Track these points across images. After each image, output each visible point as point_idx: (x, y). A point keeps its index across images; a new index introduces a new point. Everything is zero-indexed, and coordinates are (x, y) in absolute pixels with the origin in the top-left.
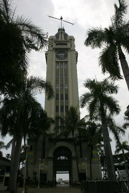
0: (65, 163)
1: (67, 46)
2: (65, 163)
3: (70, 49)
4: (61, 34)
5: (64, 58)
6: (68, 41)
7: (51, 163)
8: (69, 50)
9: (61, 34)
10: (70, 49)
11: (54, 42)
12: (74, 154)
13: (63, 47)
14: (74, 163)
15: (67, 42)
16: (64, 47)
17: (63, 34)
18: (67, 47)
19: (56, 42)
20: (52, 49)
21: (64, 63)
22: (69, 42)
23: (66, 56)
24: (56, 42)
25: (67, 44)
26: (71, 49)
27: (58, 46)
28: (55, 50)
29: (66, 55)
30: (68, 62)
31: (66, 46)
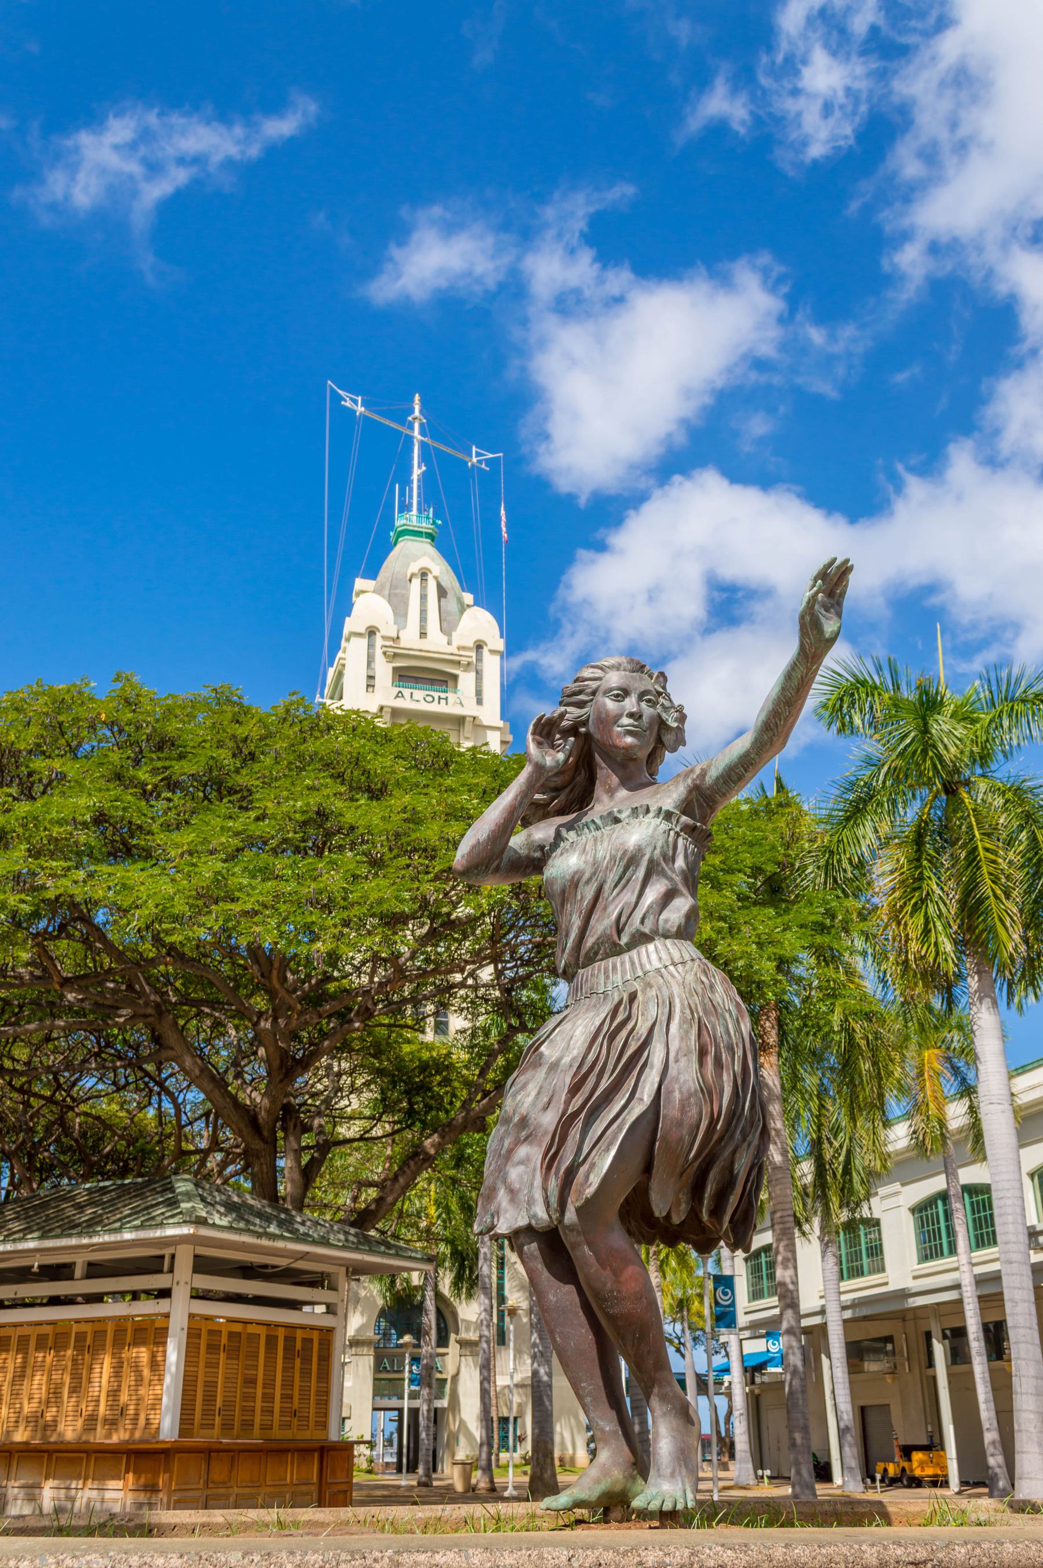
8: (468, 726)
11: (385, 653)
18: (458, 711)
19: (395, 655)
25: (455, 678)
31: (450, 696)
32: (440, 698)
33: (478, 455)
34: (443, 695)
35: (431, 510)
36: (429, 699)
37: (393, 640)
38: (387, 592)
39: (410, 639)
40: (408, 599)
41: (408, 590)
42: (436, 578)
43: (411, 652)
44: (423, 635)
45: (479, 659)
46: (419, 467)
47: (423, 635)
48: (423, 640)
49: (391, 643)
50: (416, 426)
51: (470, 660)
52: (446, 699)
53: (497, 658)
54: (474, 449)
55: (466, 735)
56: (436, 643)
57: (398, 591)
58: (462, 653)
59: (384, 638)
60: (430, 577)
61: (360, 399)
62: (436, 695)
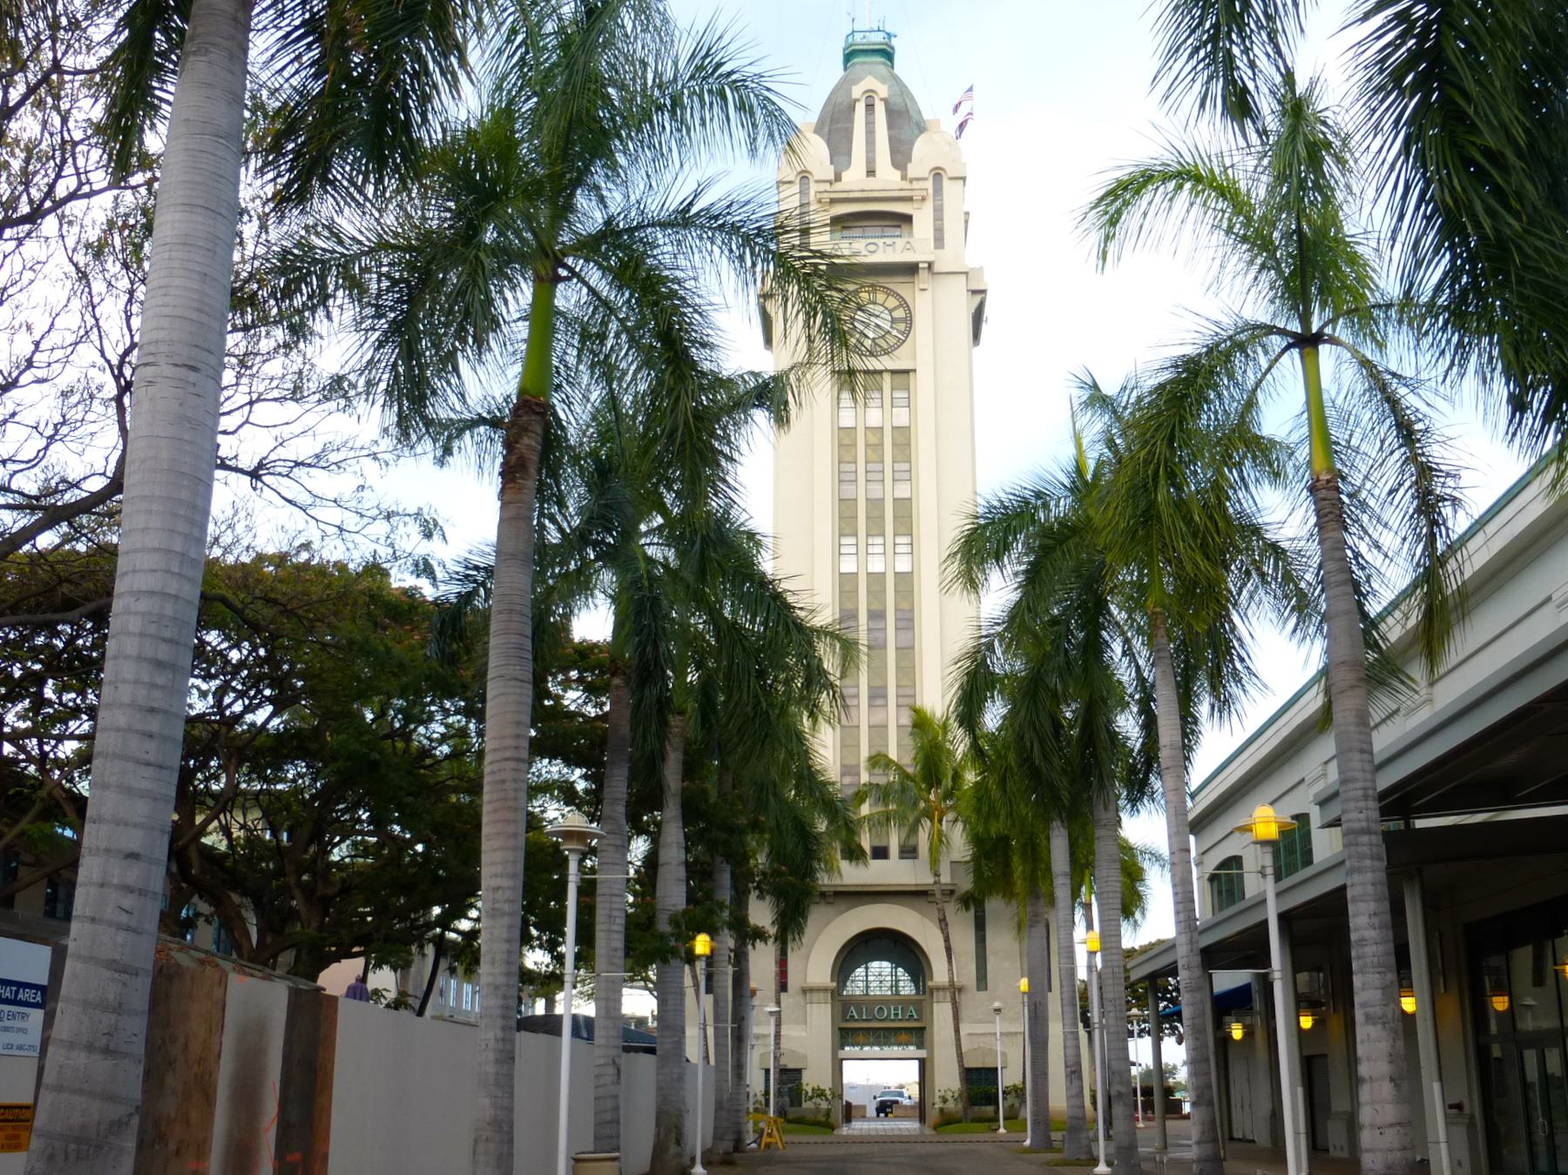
0: (896, 1015)
1: (909, 247)
2: (896, 1015)
3: (930, 265)
4: (870, 107)
6: (917, 195)
7: (821, 1016)
8: (923, 274)
9: (870, 107)
10: (930, 265)
12: (940, 973)
14: (941, 1013)
15: (910, 199)
17: (880, 109)
19: (833, 201)
21: (887, 377)
22: (923, 199)
24: (833, 201)
25: (908, 219)
26: (936, 268)
29: (900, 313)
30: (915, 371)
31: (900, 242)
34: (889, 241)
36: (872, 248)
37: (831, 183)
38: (826, 130)
39: (854, 178)
40: (851, 133)
41: (851, 121)
42: (885, 100)
43: (852, 195)
44: (871, 172)
45: (938, 190)
47: (871, 172)
48: (871, 179)
49: (827, 187)
51: (924, 193)
56: (888, 178)
57: (840, 125)
58: (916, 185)
59: (817, 182)
62: (880, 242)
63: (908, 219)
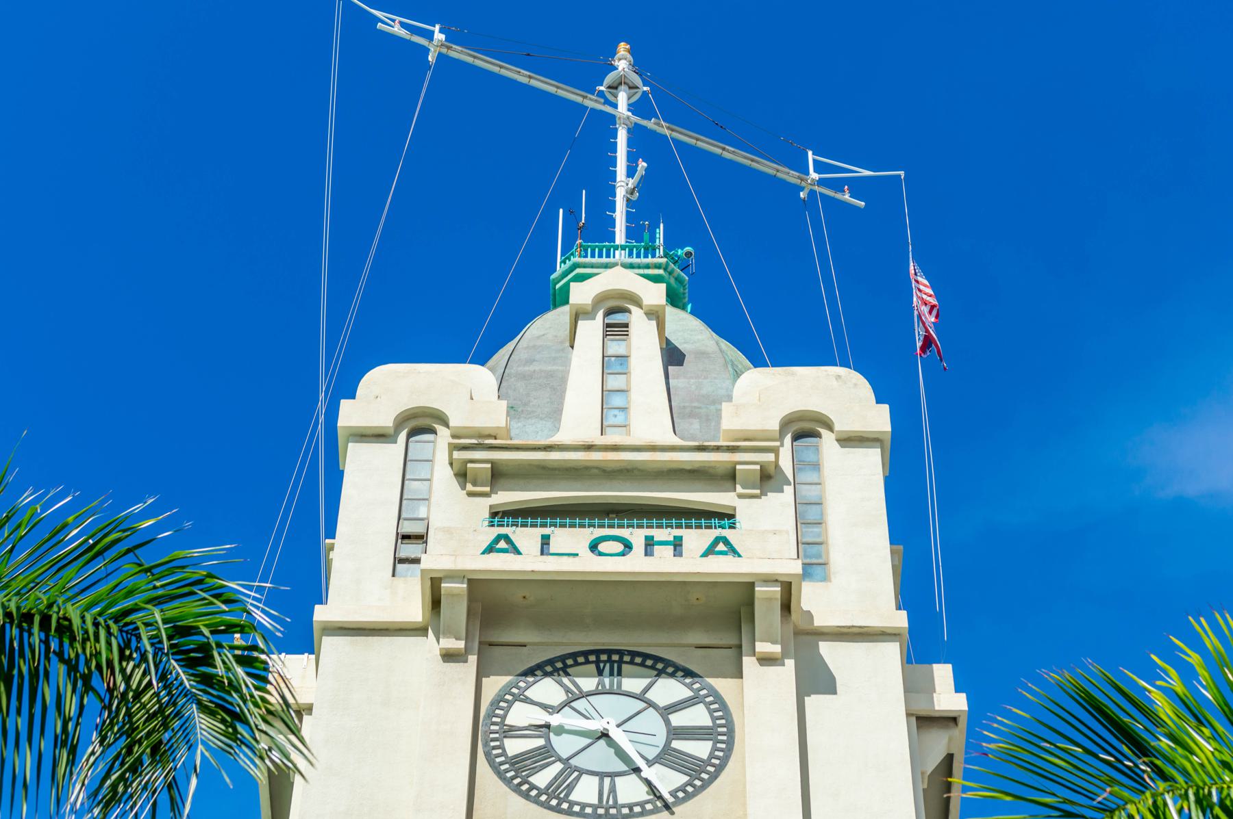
5: (668, 780)
11: (462, 475)
13: (636, 564)
15: (729, 477)
16: (663, 563)
18: (721, 566)
20: (414, 610)
23: (701, 749)
24: (499, 476)
25: (726, 517)
27: (527, 537)
28: (456, 611)
31: (696, 539)
32: (650, 544)
33: (819, 167)
35: (660, 232)
40: (563, 381)
46: (631, 172)
50: (622, 98)
52: (677, 544)
53: (871, 463)
54: (810, 153)
55: (762, 647)
60: (637, 318)
61: (437, 27)
63: (726, 517)
